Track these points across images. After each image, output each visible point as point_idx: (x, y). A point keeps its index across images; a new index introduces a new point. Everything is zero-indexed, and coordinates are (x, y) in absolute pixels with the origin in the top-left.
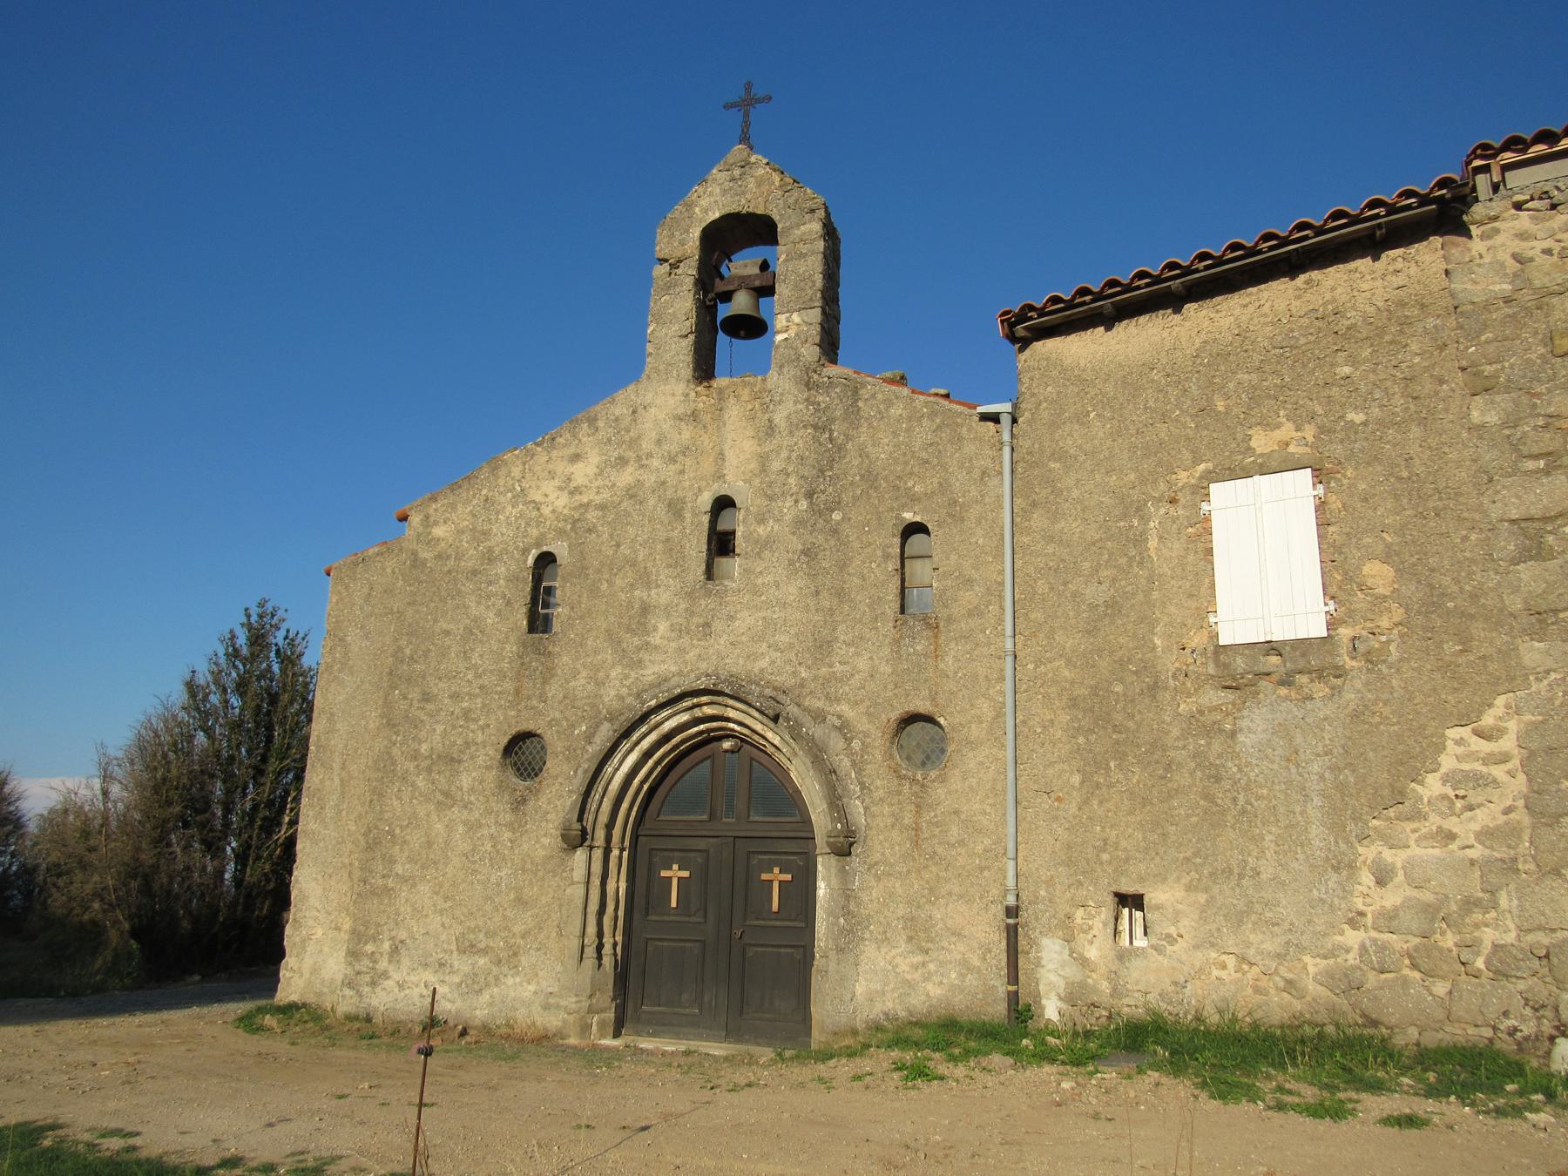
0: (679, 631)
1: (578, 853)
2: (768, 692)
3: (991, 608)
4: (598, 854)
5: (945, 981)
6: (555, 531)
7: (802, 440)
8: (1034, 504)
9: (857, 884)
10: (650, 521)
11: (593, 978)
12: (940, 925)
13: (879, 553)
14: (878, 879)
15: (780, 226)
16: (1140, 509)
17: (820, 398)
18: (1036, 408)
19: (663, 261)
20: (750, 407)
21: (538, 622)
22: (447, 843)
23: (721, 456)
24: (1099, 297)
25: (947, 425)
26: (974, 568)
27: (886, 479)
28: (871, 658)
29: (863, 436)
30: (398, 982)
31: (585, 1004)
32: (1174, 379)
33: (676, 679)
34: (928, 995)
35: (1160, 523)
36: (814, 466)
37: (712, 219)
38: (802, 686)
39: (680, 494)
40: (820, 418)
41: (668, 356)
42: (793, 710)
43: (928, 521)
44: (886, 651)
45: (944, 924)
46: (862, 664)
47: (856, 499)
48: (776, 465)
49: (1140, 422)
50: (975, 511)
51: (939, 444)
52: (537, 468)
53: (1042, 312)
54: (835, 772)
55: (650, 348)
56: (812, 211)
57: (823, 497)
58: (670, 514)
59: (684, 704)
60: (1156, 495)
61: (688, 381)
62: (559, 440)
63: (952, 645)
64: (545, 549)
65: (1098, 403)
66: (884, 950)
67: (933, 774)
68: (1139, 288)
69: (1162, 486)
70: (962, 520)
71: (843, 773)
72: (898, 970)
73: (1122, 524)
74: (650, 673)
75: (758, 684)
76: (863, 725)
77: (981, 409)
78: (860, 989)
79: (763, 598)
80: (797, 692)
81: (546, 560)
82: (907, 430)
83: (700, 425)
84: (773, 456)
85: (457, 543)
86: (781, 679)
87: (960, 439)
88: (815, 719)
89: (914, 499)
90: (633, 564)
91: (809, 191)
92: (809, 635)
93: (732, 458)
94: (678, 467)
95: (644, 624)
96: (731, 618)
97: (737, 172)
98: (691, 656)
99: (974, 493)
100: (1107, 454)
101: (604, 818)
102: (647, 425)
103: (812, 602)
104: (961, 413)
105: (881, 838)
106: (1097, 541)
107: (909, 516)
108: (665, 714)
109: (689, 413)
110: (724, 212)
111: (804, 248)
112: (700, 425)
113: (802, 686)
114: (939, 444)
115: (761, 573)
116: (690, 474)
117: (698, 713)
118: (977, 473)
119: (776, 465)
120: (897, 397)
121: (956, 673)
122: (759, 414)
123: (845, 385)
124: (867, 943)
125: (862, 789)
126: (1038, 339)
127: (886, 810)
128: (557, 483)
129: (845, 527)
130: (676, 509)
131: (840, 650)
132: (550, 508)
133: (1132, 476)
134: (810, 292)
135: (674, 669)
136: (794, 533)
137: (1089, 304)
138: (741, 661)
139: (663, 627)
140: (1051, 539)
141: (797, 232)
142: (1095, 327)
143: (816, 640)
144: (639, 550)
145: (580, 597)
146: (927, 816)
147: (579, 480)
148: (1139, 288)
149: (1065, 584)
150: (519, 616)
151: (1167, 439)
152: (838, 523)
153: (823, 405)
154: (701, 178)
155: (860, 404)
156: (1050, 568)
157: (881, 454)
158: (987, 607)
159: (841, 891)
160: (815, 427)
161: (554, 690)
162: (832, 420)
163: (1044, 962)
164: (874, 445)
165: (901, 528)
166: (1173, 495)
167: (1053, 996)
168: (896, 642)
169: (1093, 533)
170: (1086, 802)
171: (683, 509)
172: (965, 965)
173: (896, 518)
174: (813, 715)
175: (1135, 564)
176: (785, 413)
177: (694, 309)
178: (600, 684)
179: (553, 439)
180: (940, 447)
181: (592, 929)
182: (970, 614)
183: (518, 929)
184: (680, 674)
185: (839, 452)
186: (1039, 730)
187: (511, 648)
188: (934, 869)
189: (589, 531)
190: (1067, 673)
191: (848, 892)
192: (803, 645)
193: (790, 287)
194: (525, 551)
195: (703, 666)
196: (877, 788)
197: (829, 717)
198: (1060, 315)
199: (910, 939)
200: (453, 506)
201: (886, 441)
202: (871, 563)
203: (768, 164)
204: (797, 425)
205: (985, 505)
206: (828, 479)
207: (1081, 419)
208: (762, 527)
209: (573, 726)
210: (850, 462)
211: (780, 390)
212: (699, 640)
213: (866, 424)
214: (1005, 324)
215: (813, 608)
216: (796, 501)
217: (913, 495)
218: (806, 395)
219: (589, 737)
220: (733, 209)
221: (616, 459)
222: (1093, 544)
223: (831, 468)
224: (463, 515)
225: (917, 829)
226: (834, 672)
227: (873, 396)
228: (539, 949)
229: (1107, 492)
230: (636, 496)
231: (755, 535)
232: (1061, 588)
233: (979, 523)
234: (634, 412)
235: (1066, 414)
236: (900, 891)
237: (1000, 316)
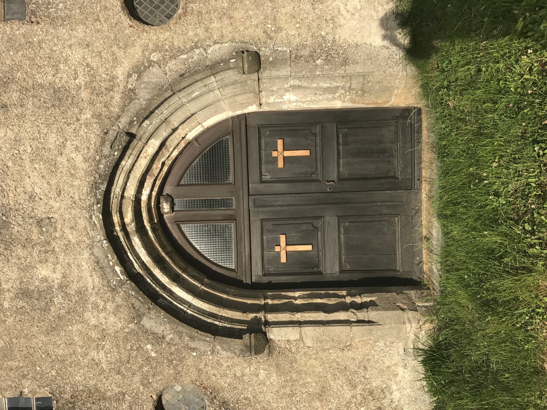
1: (272, 337)
4: (271, 317)
9: (285, 49)
14: (279, 29)
28: (70, 47)
31: (411, 314)
33: (96, 250)
42: (124, 121)
44: (62, 31)
66: (342, 21)
71: (183, 67)
72: (359, 7)
75: (99, 162)
79: (10, 164)
80: (107, 121)
88: (131, 100)
96: (32, 197)
101: (237, 315)
105: (242, 28)
117: (131, 228)
124: (337, 37)
125: (197, 47)
127: (215, 25)
135: (86, 255)
139: (43, 272)
143: (53, 106)
145: (11, 370)
168: (53, 21)
181: (341, 316)
183: (348, 394)
184: (91, 247)
191: (293, 56)
192: (59, 119)
195: (82, 223)
196: (196, 35)
197: (130, 86)
209: (148, 359)
215: (20, 110)
219: (159, 339)
226: (86, 84)
228: (365, 368)
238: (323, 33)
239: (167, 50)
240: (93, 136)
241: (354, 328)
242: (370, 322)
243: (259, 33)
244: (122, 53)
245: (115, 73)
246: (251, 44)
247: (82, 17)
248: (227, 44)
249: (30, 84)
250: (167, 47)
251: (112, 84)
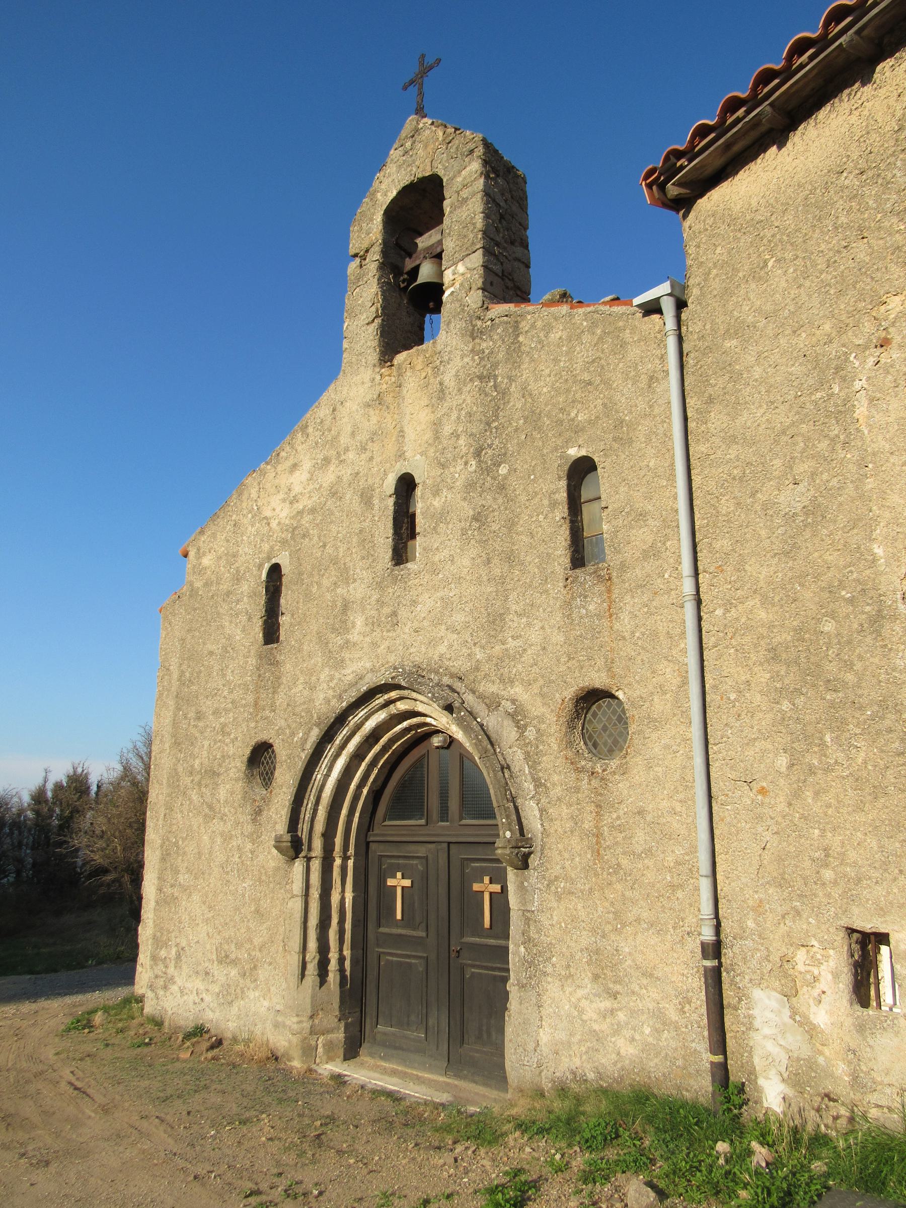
0: (373, 624)
2: (446, 680)
3: (668, 544)
5: (637, 1037)
6: (279, 542)
7: (469, 398)
8: (711, 400)
10: (347, 516)
11: (313, 997)
12: (629, 962)
13: (546, 502)
14: (559, 899)
15: (445, 180)
16: (841, 370)
17: (484, 345)
18: (705, 280)
19: (356, 255)
20: (424, 375)
21: (271, 633)
22: (210, 853)
23: (402, 434)
24: (753, 101)
25: (609, 333)
26: (645, 498)
27: (549, 416)
28: (543, 628)
29: (526, 372)
30: (180, 987)
31: (307, 1025)
32: (870, 174)
33: (370, 675)
34: (619, 1054)
35: (868, 379)
36: (481, 420)
37: (391, 198)
38: (477, 669)
39: (370, 481)
40: (485, 366)
41: (358, 347)
42: (469, 698)
43: (594, 453)
44: (558, 617)
45: (633, 961)
46: (535, 636)
47: (521, 445)
48: (447, 429)
49: (830, 250)
50: (642, 430)
51: (600, 359)
52: (268, 486)
53: (689, 153)
54: (508, 767)
55: (345, 344)
56: (472, 152)
57: (490, 452)
58: (362, 505)
59: (377, 702)
60: (860, 342)
61: (375, 366)
62: (283, 454)
63: (628, 598)
64: (274, 561)
65: (776, 245)
66: (568, 990)
67: (614, 763)
68: (802, 67)
69: (868, 327)
70: (630, 441)
71: (517, 769)
72: (585, 1017)
73: (819, 395)
74: (349, 672)
75: (437, 672)
76: (536, 708)
77: (637, 301)
78: (544, 1037)
79: (441, 576)
80: (471, 678)
81: (275, 571)
82: (567, 353)
83: (385, 407)
84: (445, 420)
85: (217, 570)
86: (460, 665)
87: (624, 344)
88: (488, 706)
89: (578, 430)
90: (335, 561)
91: (468, 133)
92: (482, 610)
93: (411, 434)
94: (368, 454)
95: (345, 622)
96: (414, 603)
97: (408, 145)
98: (382, 649)
99: (642, 405)
100: (792, 308)
101: (320, 826)
102: (344, 420)
103: (483, 572)
104: (623, 314)
105: (560, 846)
106: (788, 427)
107: (574, 452)
108: (362, 713)
109: (375, 397)
110: (399, 188)
111: (465, 194)
112: (385, 407)
113: (477, 669)
114: (600, 359)
115: (437, 549)
116: (377, 459)
117: (392, 709)
118: (644, 379)
119: (447, 429)
120: (556, 319)
121: (633, 633)
122: (432, 380)
123: (506, 323)
124: (549, 979)
125: (536, 787)
126: (701, 195)
127: (565, 811)
128: (281, 496)
129: (513, 482)
130: (366, 498)
131: (514, 623)
132: (277, 521)
133: (827, 327)
134: (471, 236)
135: (368, 665)
136: (465, 499)
137: (744, 117)
138: (423, 649)
139: (359, 622)
140: (733, 440)
141: (459, 179)
142: (765, 151)
143: (489, 614)
144: (339, 547)
145: (297, 603)
146: (608, 818)
147: (297, 489)
148: (802, 67)
149: (753, 495)
150: (257, 629)
151: (867, 259)
152: (505, 478)
153: (487, 351)
154: (380, 165)
155: (521, 339)
156: (734, 479)
157: (542, 388)
158: (664, 544)
159: (520, 913)
160: (481, 378)
161: (281, 699)
162: (495, 366)
163: (757, 1023)
164: (536, 381)
165: (566, 468)
166: (884, 334)
167: (772, 1073)
168: (568, 604)
169: (783, 417)
170: (797, 794)
171: (372, 496)
172: (659, 1015)
173: (561, 457)
174: (487, 701)
175: (838, 447)
176: (453, 372)
177: (380, 293)
178: (312, 688)
179: (278, 455)
180: (603, 362)
181: (312, 945)
182: (646, 555)
183: (257, 941)
185: (503, 398)
186: (733, 696)
187: (253, 661)
188: (618, 886)
189: (304, 536)
190: (762, 614)
191: (528, 915)
192: (477, 623)
193: (455, 238)
194: (260, 566)
195: (392, 659)
196: (554, 785)
197: (503, 702)
198: (712, 149)
199: (596, 977)
200: (214, 535)
201: (547, 371)
202: (538, 515)
203: (433, 123)
204: (465, 380)
205: (655, 416)
206: (494, 430)
207: (758, 273)
208: (437, 499)
209: (293, 734)
210: (514, 406)
211: (449, 348)
212: (388, 631)
213: (527, 359)
214: (654, 188)
215: (485, 578)
216: (466, 463)
217: (577, 426)
218: (471, 346)
220: (406, 181)
221: (322, 460)
222: (784, 432)
223: (497, 417)
224: (220, 546)
225: (598, 835)
226: (507, 650)
227: (533, 326)
228: (270, 964)
229: (797, 358)
230: (336, 493)
231: (432, 509)
232: (749, 501)
233: (648, 441)
234: (334, 410)
235: (741, 274)
236: (582, 914)
237: (645, 179)
238: (554, 959)
239: (538, 747)
240: (460, 663)
241: (297, 956)
242: (303, 975)
243: (556, 870)
244: (536, 691)
245: (517, 683)
246: (540, 858)
247: (572, 639)
248: (539, 826)
249: (509, 587)
250: (541, 747)
251: (506, 681)
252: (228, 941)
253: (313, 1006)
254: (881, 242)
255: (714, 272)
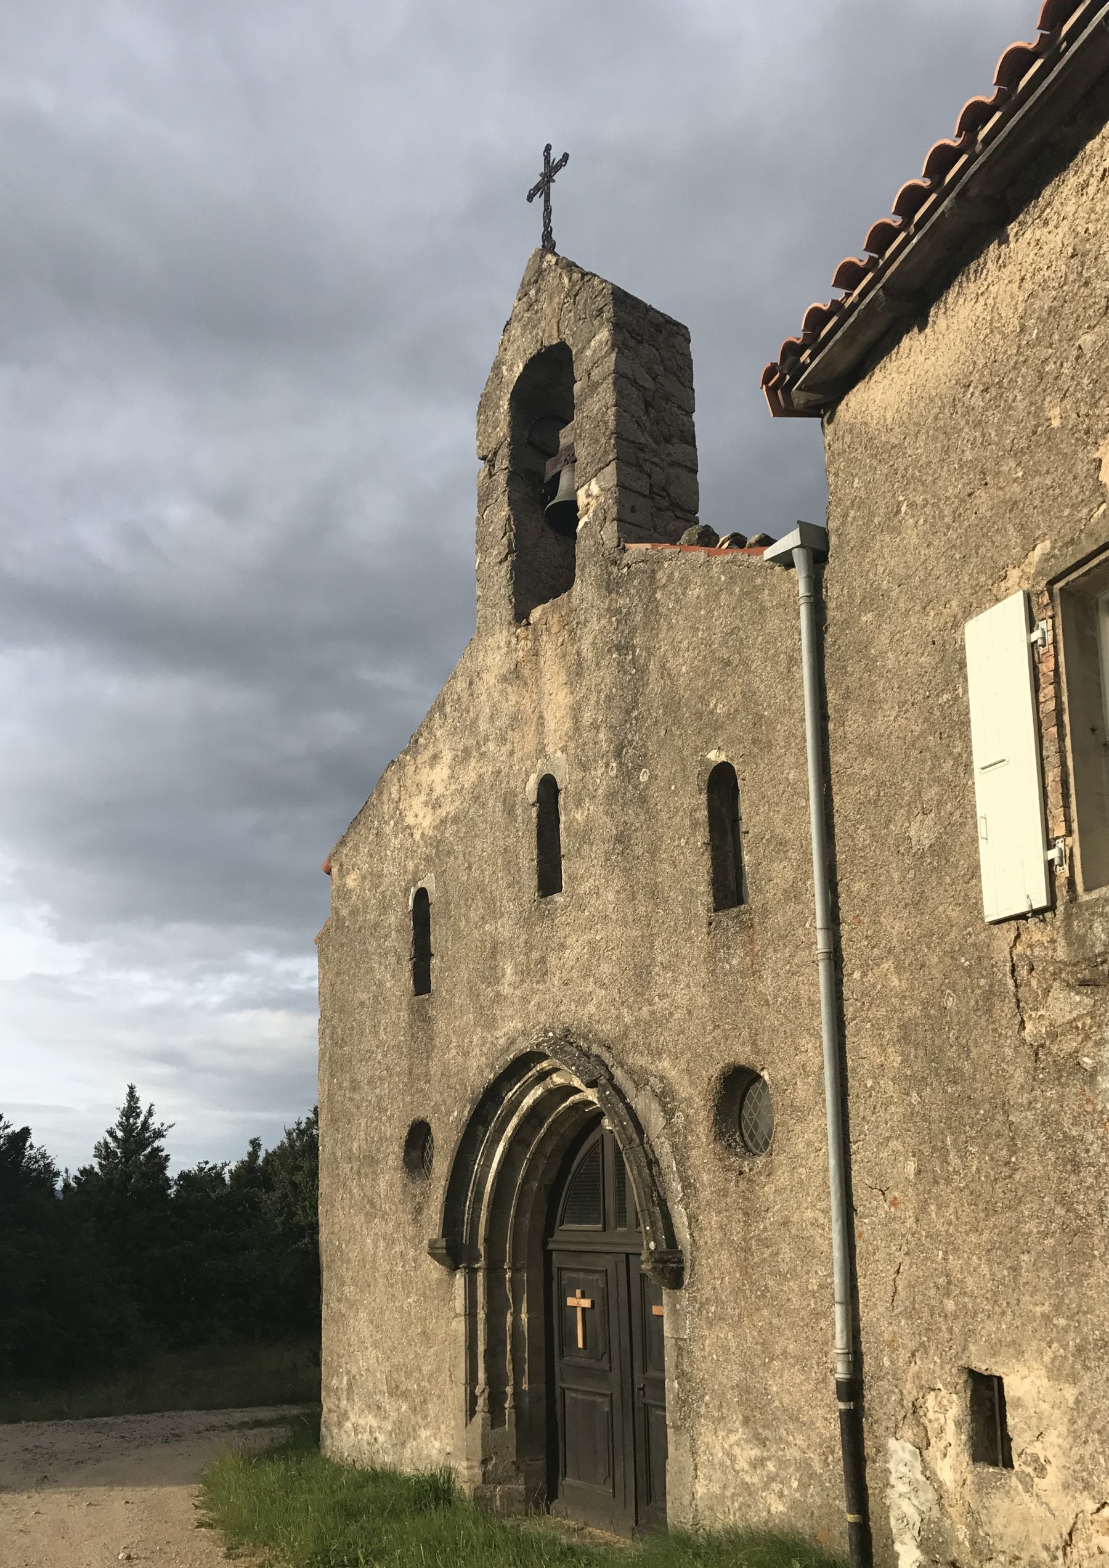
0: (524, 972)
1: (458, 1276)
5: (786, 1492)
9: (688, 1331)
11: (484, 1437)
12: (777, 1403)
13: (687, 822)
20: (561, 640)
21: (422, 982)
22: (374, 1261)
30: (353, 1424)
34: (769, 1512)
45: (781, 1403)
46: (680, 996)
48: (587, 717)
51: (739, 629)
54: (657, 1162)
61: (510, 623)
64: (420, 885)
66: (721, 1434)
67: (760, 1161)
70: (770, 745)
72: (737, 1467)
74: (501, 1035)
75: (586, 1039)
76: (684, 1090)
78: (700, 1490)
79: (587, 913)
81: (422, 895)
86: (608, 1029)
87: (762, 610)
92: (629, 959)
94: (508, 746)
96: (562, 946)
107: (715, 756)
114: (739, 629)
116: (518, 755)
121: (776, 997)
128: (423, 798)
131: (661, 978)
143: (635, 965)
146: (757, 1228)
147: (439, 789)
155: (658, 595)
157: (682, 666)
158: (804, 883)
159: (673, 1341)
160: (619, 648)
162: (633, 631)
163: (893, 1480)
164: (674, 656)
165: (706, 777)
167: (907, 1537)
168: (711, 955)
170: (923, 1208)
171: (514, 806)
172: (804, 1465)
174: (636, 1077)
176: (590, 640)
178: (466, 1054)
183: (426, 1369)
184: (525, 1033)
186: (869, 1083)
187: (404, 1015)
188: (765, 1312)
190: (895, 982)
194: (406, 891)
199: (746, 1421)
200: (356, 848)
202: (680, 839)
206: (634, 722)
208: (580, 812)
209: (449, 1113)
212: (538, 982)
217: (717, 721)
225: (747, 1250)
227: (670, 577)
230: (478, 797)
234: (471, 683)
236: (733, 1344)
238: (707, 1398)
239: (686, 1138)
240: (609, 1027)
241: (464, 1388)
242: (471, 1412)
243: (708, 1292)
244: (682, 1067)
245: (664, 1056)
246: (690, 1275)
247: (717, 1001)
248: (688, 1236)
249: (655, 931)
250: (689, 1138)
251: (655, 1052)
252: (397, 1368)
253: (483, 1449)
254: (1000, 493)
255: (852, 513)
